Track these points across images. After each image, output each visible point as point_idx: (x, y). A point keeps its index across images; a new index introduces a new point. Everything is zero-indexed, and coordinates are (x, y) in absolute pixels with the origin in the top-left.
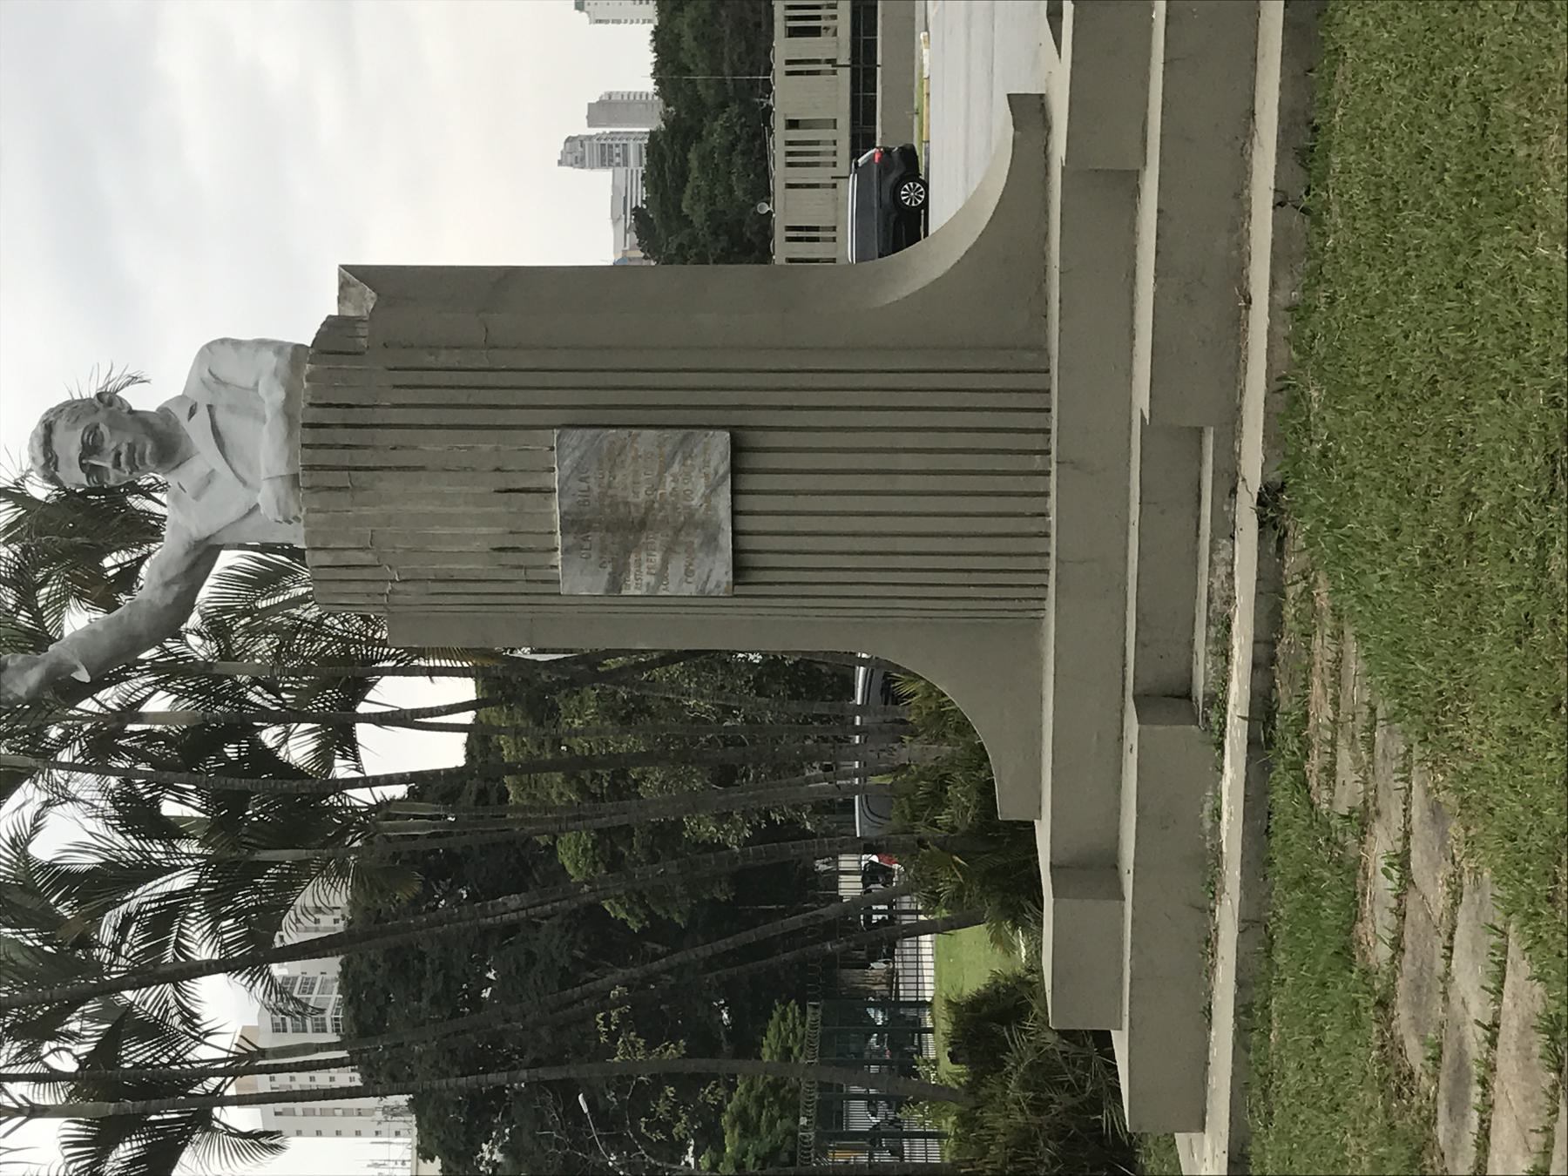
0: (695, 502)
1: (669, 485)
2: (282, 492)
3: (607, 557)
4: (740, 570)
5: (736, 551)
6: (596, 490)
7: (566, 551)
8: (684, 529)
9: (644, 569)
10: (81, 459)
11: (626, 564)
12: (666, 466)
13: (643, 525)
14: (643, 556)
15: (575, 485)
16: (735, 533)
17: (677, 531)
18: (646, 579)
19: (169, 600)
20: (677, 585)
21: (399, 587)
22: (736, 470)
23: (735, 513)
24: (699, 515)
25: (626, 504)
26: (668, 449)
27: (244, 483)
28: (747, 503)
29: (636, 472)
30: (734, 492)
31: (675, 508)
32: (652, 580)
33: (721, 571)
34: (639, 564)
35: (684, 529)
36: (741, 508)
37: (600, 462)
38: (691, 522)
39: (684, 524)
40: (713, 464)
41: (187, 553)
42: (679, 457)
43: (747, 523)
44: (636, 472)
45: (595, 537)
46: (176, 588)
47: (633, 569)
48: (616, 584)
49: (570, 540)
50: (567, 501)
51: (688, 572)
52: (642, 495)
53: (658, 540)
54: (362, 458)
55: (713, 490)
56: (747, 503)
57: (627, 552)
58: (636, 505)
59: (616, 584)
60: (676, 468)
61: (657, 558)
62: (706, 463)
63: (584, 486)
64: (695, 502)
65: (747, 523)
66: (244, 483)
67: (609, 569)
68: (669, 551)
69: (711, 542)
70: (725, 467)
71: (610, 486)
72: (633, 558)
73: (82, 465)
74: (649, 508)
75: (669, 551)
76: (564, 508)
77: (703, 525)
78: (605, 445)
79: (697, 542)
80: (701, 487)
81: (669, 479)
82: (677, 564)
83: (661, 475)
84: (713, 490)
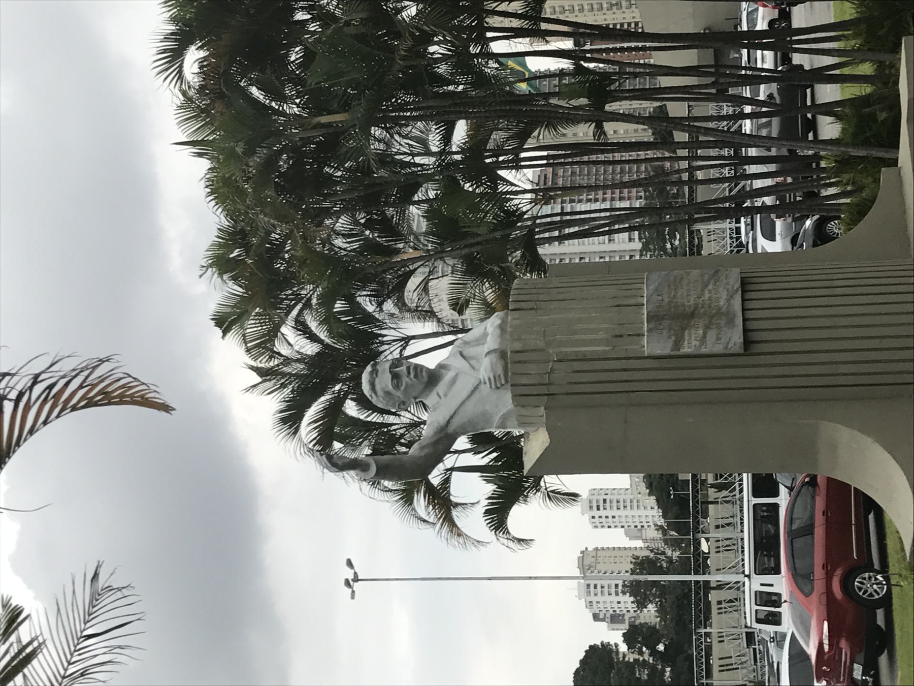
0: (722, 303)
1: (707, 296)
2: (494, 360)
3: (672, 332)
4: (748, 343)
5: (746, 331)
6: (666, 300)
7: (649, 331)
8: (715, 317)
9: (693, 338)
10: (390, 368)
11: (683, 336)
12: (707, 286)
13: (692, 315)
14: (693, 331)
15: (656, 298)
16: (745, 320)
17: (713, 317)
18: (694, 343)
19: (423, 454)
20: (712, 346)
21: (557, 366)
22: (744, 291)
23: (744, 310)
24: (724, 309)
25: (683, 305)
26: (706, 277)
27: (473, 368)
28: (750, 305)
29: (689, 290)
30: (743, 300)
31: (710, 307)
32: (697, 343)
33: (736, 337)
34: (690, 335)
35: (715, 317)
36: (747, 317)
37: (669, 286)
38: (719, 313)
39: (716, 314)
40: (731, 282)
41: (436, 433)
42: (712, 281)
43: (750, 315)
44: (689, 290)
45: (666, 323)
46: (426, 451)
47: (686, 337)
48: (677, 345)
49: (652, 325)
50: (650, 307)
51: (718, 339)
52: (692, 302)
53: (701, 323)
54: (541, 297)
55: (731, 296)
56: (750, 305)
57: (683, 329)
58: (690, 306)
59: (677, 345)
60: (710, 287)
61: (701, 332)
62: (727, 284)
63: (660, 298)
64: (722, 303)
65: (750, 315)
66: (473, 368)
67: (673, 338)
68: (707, 328)
69: (731, 322)
70: (738, 285)
71: (674, 296)
72: (687, 332)
73: (390, 372)
74: (696, 306)
75: (707, 328)
76: (649, 309)
77: (727, 314)
78: (672, 278)
79: (723, 322)
80: (724, 296)
81: (707, 292)
82: (711, 335)
83: (702, 290)
84: (731, 296)
